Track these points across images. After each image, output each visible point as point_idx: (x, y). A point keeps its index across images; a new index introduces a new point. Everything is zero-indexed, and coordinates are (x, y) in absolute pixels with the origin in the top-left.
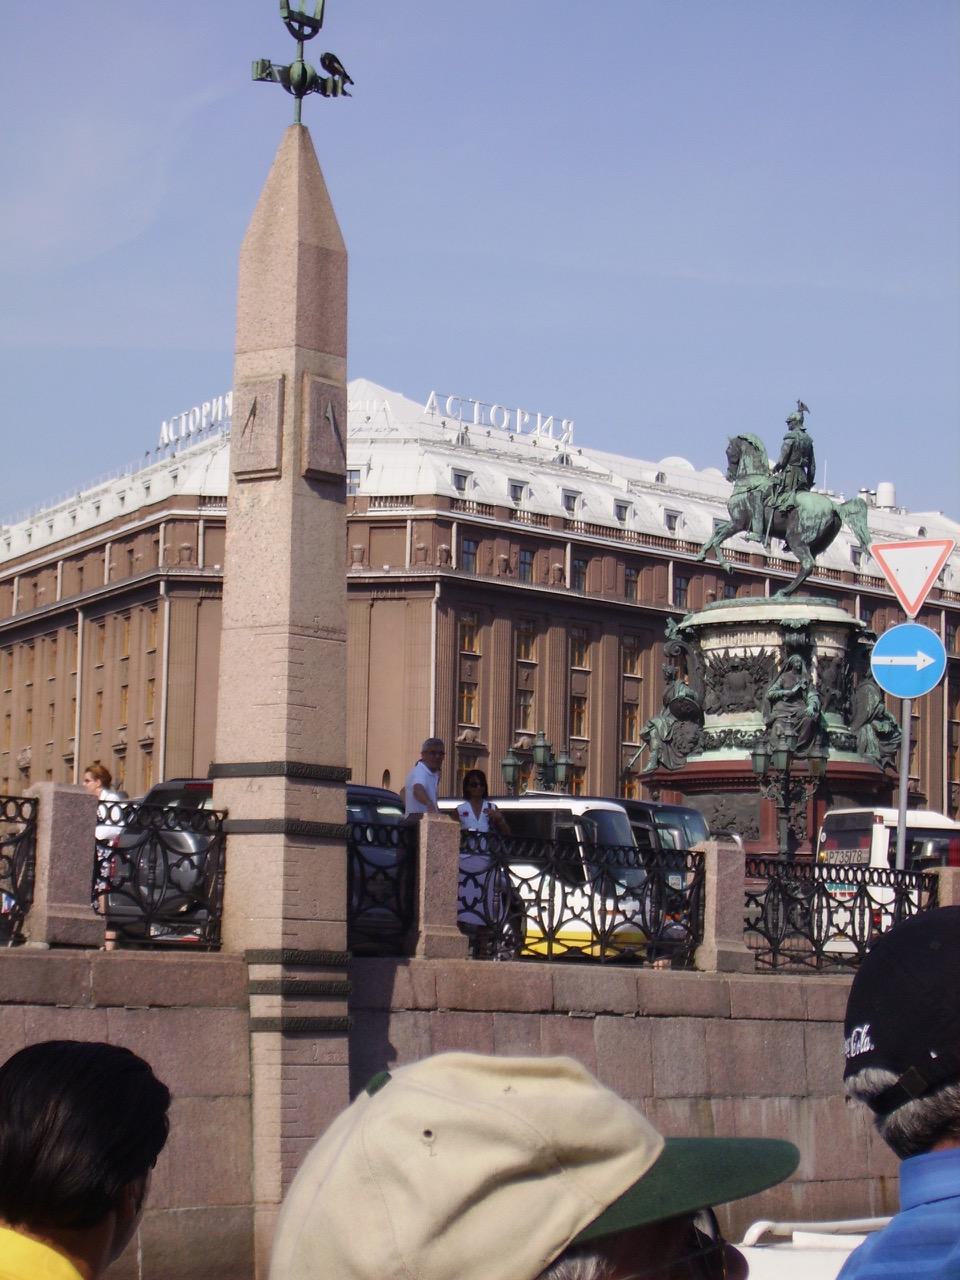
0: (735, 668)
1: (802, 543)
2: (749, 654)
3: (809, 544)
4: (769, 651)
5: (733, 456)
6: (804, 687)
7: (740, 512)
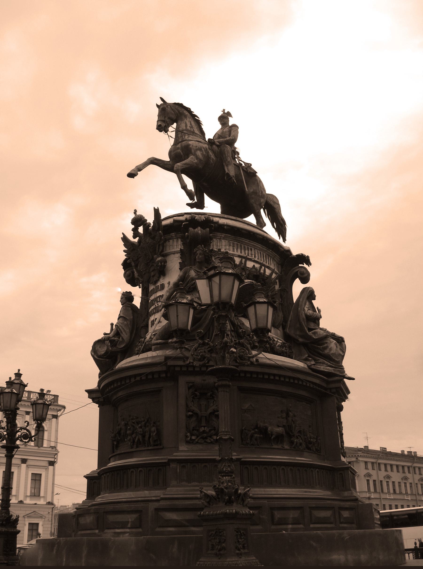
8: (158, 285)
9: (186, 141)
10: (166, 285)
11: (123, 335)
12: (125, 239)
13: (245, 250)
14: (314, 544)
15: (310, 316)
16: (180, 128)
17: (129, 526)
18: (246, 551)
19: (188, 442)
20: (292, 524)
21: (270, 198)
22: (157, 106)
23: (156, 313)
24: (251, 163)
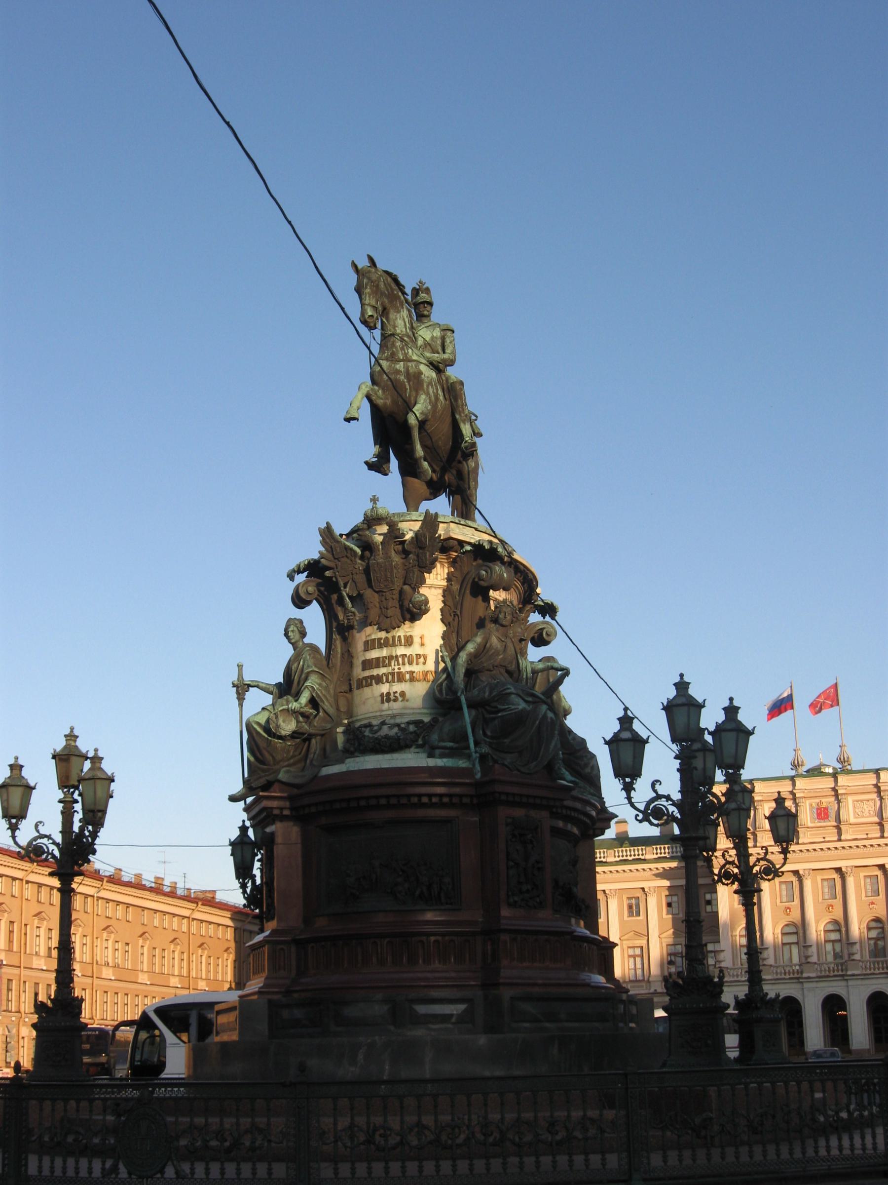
8: (398, 634)
9: (415, 363)
10: (417, 640)
11: (325, 707)
12: (327, 533)
16: (397, 328)
17: (454, 1020)
19: (510, 905)
22: (355, 266)
23: (396, 683)
24: (477, 415)
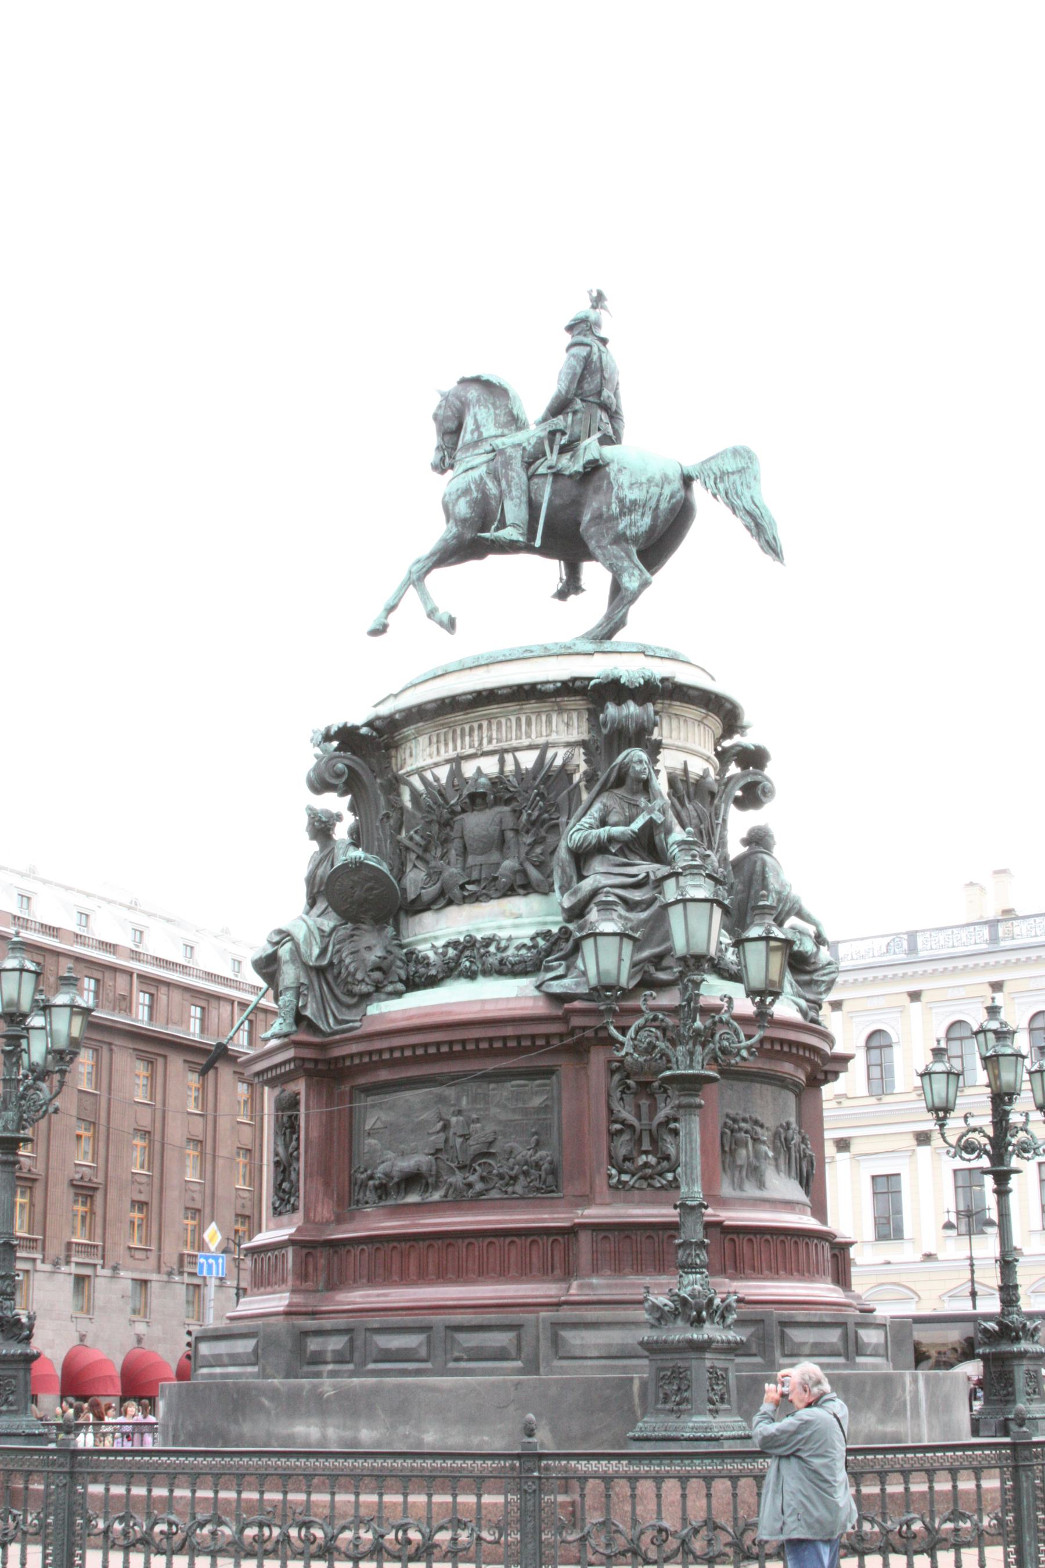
0: (476, 800)
1: (620, 539)
2: (510, 767)
3: (635, 540)
4: (558, 757)
5: (446, 418)
6: (658, 817)
7: (474, 504)
13: (454, 741)
14: (266, 1402)
15: (579, 848)
18: (14, 1408)
20: (335, 1362)
21: (711, 469)
